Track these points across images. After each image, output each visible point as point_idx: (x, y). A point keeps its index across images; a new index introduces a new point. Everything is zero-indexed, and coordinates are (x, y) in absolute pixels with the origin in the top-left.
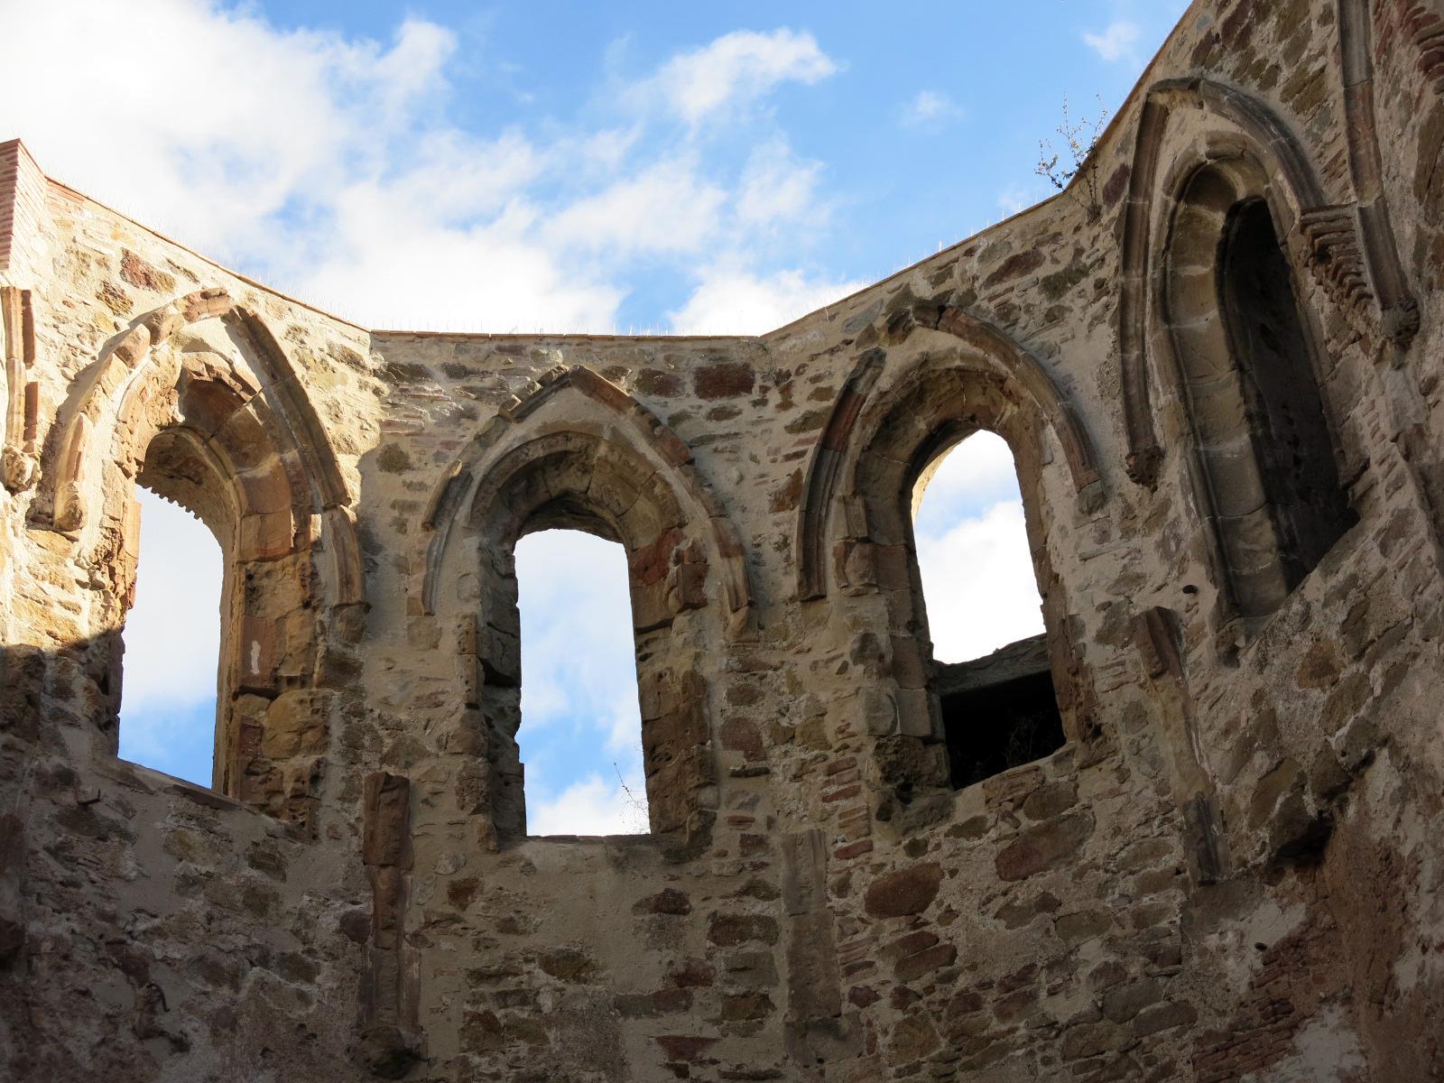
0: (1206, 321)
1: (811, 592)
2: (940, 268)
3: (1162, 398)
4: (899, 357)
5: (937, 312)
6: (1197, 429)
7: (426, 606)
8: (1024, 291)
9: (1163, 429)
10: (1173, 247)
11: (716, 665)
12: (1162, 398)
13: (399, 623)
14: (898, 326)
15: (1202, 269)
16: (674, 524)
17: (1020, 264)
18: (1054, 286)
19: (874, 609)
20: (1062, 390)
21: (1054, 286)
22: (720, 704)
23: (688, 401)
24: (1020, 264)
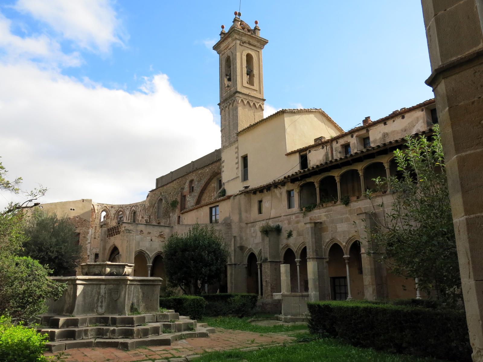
0: (132, 215)
1: (114, 219)
2: (123, 205)
3: (130, 217)
4: (120, 209)
5: (122, 208)
6: (131, 220)
7: (98, 218)
8: (126, 208)
9: (130, 219)
10: (132, 211)
11: (109, 222)
12: (130, 217)
13: (97, 218)
14: (120, 208)
15: (133, 213)
16: (108, 215)
17: (126, 207)
18: (127, 209)
19: (116, 221)
20: (126, 214)
21: (127, 209)
22: (109, 224)
23: (110, 208)
24: (126, 207)
